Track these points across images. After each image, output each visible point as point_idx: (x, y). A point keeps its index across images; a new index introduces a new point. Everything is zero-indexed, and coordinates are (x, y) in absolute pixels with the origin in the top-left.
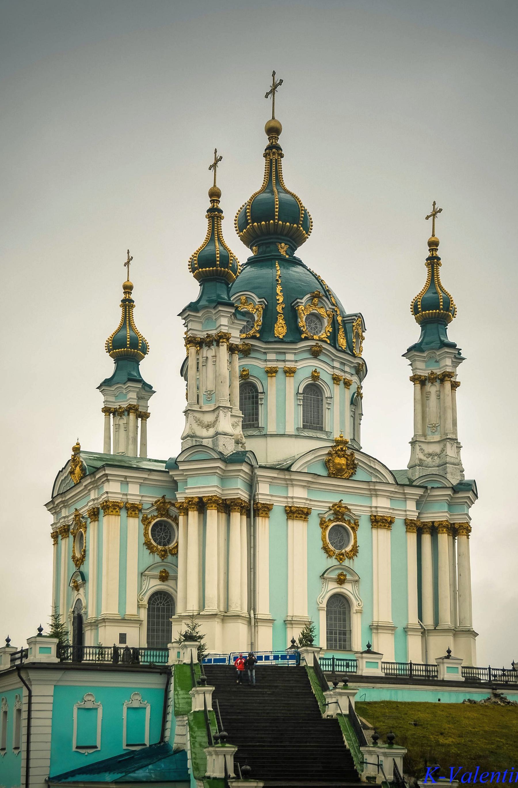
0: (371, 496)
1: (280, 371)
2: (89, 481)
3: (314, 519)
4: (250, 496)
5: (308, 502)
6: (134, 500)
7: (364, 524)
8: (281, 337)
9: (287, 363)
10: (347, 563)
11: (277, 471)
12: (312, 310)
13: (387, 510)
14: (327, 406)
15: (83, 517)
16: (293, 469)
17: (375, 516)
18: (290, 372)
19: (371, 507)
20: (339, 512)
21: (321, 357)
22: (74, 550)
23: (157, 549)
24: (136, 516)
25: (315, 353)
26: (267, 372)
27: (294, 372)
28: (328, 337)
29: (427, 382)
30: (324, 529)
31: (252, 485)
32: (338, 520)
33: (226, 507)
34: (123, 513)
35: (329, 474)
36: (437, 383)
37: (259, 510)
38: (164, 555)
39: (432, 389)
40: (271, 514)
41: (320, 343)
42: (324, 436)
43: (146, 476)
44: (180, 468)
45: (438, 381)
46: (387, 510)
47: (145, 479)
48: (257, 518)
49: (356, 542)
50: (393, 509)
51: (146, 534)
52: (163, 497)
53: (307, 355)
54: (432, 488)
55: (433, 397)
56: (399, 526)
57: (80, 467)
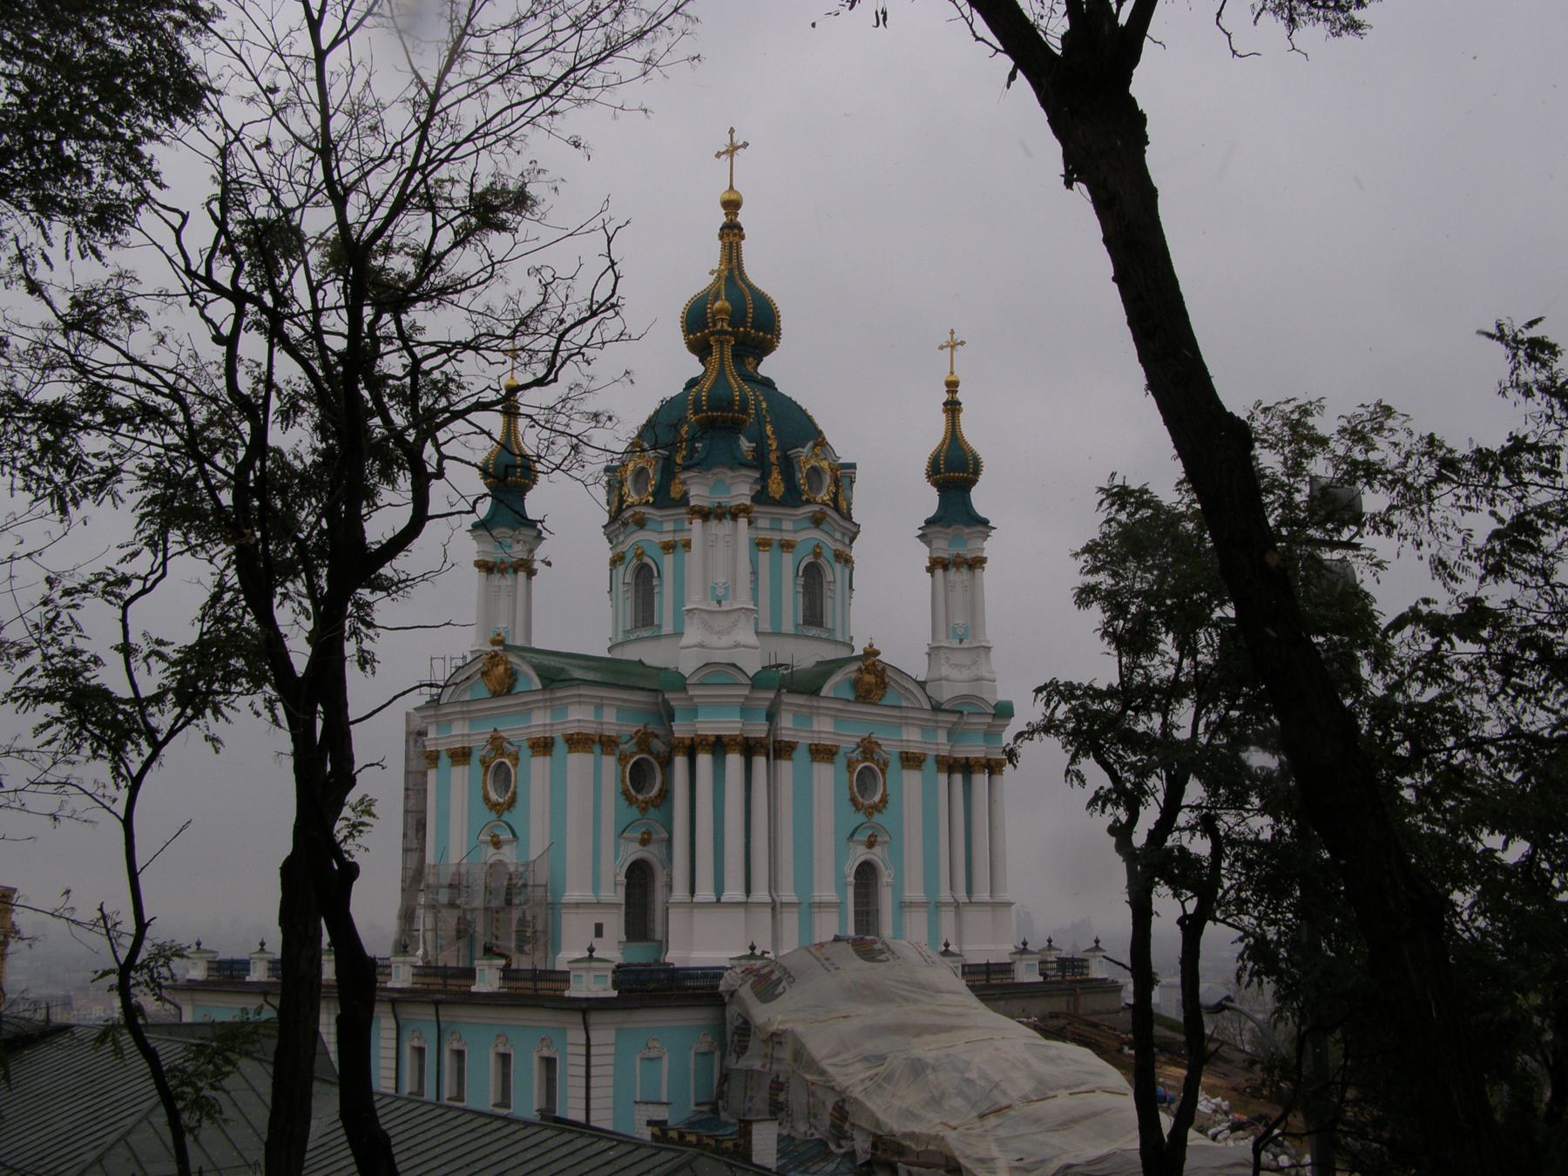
1: (775, 545)
3: (841, 760)
6: (610, 731)
7: (895, 764)
10: (877, 818)
12: (813, 462)
18: (787, 546)
20: (868, 748)
21: (823, 526)
25: (817, 521)
26: (758, 544)
30: (851, 773)
31: (771, 716)
32: (865, 759)
34: (597, 748)
36: (964, 570)
39: (958, 577)
40: (795, 755)
47: (625, 700)
51: (623, 781)
56: (930, 764)
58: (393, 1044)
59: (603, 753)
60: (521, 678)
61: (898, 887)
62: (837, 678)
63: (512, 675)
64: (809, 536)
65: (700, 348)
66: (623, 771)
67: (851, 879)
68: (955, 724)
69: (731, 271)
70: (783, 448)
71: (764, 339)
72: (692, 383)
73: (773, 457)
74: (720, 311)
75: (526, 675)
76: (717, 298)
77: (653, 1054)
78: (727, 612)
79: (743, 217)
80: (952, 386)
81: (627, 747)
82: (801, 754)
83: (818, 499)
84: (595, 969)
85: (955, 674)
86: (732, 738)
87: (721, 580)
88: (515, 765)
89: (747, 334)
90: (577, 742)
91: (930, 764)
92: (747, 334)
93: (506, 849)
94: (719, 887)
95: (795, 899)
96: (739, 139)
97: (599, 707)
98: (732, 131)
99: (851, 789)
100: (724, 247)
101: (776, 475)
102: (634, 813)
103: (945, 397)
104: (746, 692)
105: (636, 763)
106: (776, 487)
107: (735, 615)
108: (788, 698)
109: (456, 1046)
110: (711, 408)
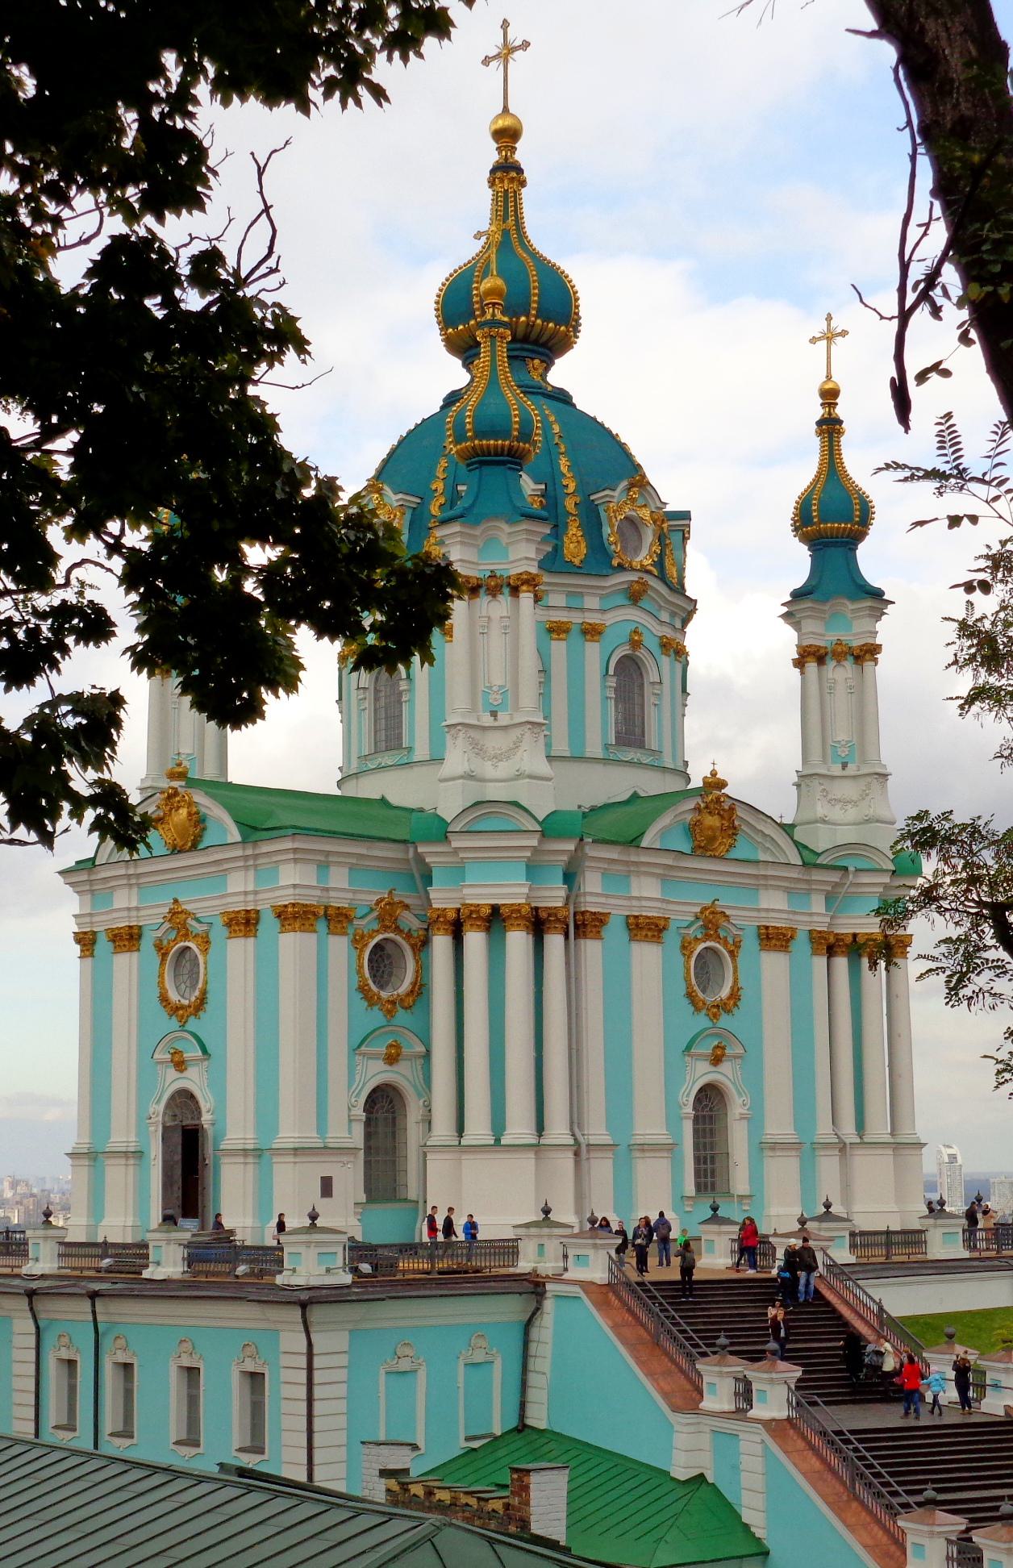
0: (757, 888)
1: (575, 629)
2: (239, 853)
3: (672, 938)
4: (568, 898)
5: (664, 906)
6: (338, 901)
7: (750, 943)
8: (577, 561)
9: (587, 614)
10: (725, 1021)
11: (619, 848)
13: (785, 916)
14: (653, 699)
15: (197, 920)
16: (644, 844)
17: (767, 928)
18: (592, 632)
19: (759, 910)
20: (712, 921)
22: (161, 984)
23: (379, 998)
24: (344, 934)
25: (635, 596)
26: (550, 630)
27: (600, 633)
28: (654, 564)
29: (828, 658)
32: (707, 937)
33: (538, 924)
34: (321, 926)
35: (694, 849)
36: (849, 663)
37: (585, 925)
38: (391, 1007)
39: (840, 673)
40: (606, 932)
41: (647, 577)
42: (646, 760)
43: (364, 851)
44: (455, 844)
45: (851, 659)
46: (785, 916)
48: (582, 941)
49: (736, 981)
50: (795, 913)
51: (360, 971)
52: (390, 893)
53: (621, 600)
54: (857, 870)
55: (841, 691)
56: (801, 944)
57: (190, 814)
58: (31, 1355)
59: (331, 932)
60: (209, 824)
61: (754, 1120)
62: (665, 820)
63: (199, 821)
64: (621, 619)
65: (464, 348)
66: (360, 957)
67: (689, 1110)
68: (836, 885)
69: (505, 233)
70: (585, 491)
71: (555, 333)
72: (452, 399)
73: (570, 504)
74: (490, 292)
75: (219, 821)
76: (486, 273)
77: (405, 1365)
78: (505, 728)
79: (523, 154)
80: (830, 396)
81: (367, 924)
82: (615, 930)
83: (636, 564)
84: (318, 1244)
85: (836, 814)
86: (515, 909)
87: (498, 679)
88: (205, 951)
89: (530, 326)
90: (295, 917)
91: (801, 944)
92: (530, 326)
93: (192, 1072)
94: (498, 1124)
95: (607, 1140)
96: (516, 36)
97: (323, 866)
98: (505, 25)
99: (687, 979)
100: (495, 200)
101: (573, 530)
102: (377, 1017)
103: (819, 413)
104: (534, 842)
105: (378, 946)
106: (575, 546)
107: (518, 732)
108: (592, 851)
109: (122, 1358)
110: (479, 434)
